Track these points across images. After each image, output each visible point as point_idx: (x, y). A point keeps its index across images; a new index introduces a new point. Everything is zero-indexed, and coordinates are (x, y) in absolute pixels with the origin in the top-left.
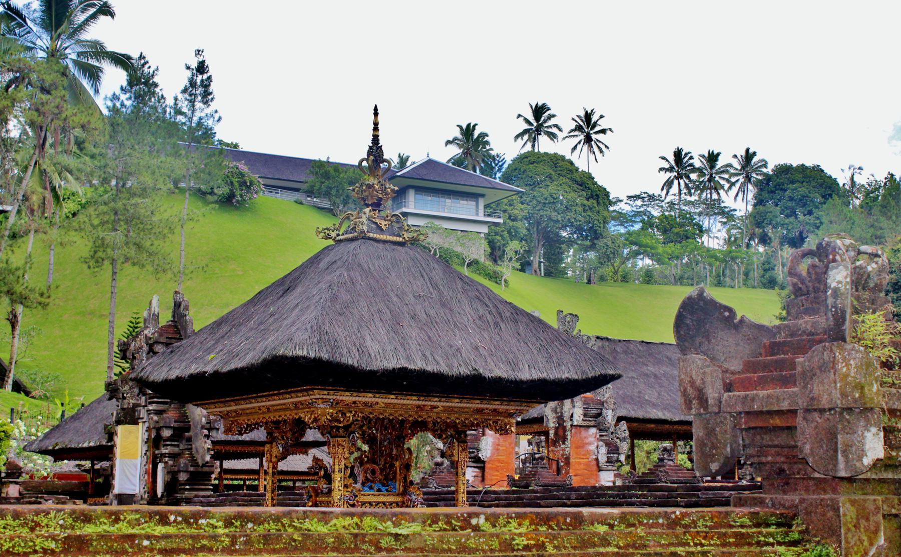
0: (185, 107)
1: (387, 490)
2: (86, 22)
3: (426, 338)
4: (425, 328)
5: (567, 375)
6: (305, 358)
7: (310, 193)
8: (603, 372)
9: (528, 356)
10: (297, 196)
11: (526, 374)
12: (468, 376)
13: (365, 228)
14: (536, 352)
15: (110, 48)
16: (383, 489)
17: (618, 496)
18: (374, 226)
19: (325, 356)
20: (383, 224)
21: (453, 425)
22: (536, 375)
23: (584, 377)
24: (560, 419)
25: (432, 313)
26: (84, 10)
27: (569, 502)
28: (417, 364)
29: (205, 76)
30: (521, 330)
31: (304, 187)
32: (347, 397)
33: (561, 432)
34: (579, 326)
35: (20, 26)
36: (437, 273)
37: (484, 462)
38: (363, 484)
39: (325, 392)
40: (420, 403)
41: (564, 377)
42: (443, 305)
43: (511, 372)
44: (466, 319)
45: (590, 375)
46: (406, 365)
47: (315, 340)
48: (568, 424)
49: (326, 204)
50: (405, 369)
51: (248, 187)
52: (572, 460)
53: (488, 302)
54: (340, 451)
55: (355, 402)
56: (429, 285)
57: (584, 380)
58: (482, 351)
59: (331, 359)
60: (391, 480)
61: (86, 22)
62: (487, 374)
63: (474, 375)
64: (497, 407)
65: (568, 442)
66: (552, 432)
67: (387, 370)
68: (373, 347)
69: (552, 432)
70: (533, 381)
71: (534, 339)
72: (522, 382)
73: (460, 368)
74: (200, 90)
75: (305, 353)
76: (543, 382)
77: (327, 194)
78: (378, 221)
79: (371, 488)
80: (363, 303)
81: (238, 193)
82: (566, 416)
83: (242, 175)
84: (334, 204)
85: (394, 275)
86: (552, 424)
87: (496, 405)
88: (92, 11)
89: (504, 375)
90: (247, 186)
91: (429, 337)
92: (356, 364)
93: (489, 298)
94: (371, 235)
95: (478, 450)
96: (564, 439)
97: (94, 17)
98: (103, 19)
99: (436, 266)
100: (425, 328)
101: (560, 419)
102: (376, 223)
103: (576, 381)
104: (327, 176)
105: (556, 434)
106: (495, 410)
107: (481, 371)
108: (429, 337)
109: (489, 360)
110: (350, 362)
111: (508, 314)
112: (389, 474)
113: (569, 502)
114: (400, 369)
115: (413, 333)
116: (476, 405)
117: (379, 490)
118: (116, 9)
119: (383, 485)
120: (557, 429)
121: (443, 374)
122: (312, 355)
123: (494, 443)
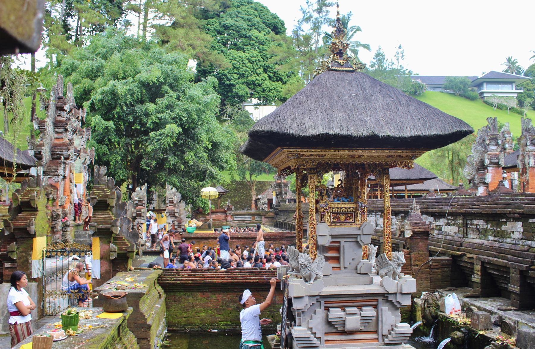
0: (395, 61)
1: (348, 201)
2: (352, 35)
3: (347, 117)
4: (349, 112)
5: (435, 133)
6: (262, 131)
7: (446, 88)
8: (459, 130)
9: (411, 123)
10: (440, 90)
11: (407, 133)
12: (368, 136)
13: (330, 65)
14: (416, 121)
15: (362, 43)
16: (346, 200)
17: (510, 199)
18: (336, 64)
19: (274, 129)
20: (342, 62)
21: (380, 165)
22: (414, 133)
23: (446, 133)
24: (524, 164)
25: (357, 103)
26: (352, 31)
27: (487, 203)
28: (336, 130)
29: (401, 50)
30: (411, 109)
31: (443, 86)
32: (306, 152)
33: (524, 170)
34: (531, 123)
35: (330, 39)
36: (367, 83)
37: (488, 184)
38: (334, 198)
39: (291, 150)
40: (351, 154)
41: (432, 134)
42: (366, 99)
43: (397, 133)
44: (378, 106)
45: (450, 132)
46: (327, 132)
47: (270, 121)
48: (527, 166)
49: (452, 92)
50: (326, 134)
51: (422, 88)
52: (530, 182)
53: (394, 97)
54: (312, 181)
55: (311, 155)
56: (360, 90)
57: (446, 135)
58: (381, 122)
59: (279, 130)
60: (351, 195)
61: (352, 35)
62: (381, 134)
63: (372, 136)
64: (400, 154)
65: (528, 174)
66: (521, 170)
67: (315, 135)
68: (308, 122)
69: (521, 170)
70: (411, 137)
71: (418, 114)
72: (404, 138)
73: (364, 132)
74: (400, 55)
75: (263, 128)
76: (418, 138)
77: (452, 88)
78: (339, 61)
79: (339, 200)
80: (313, 102)
81: (418, 91)
82: (526, 163)
83: (419, 84)
84: (455, 91)
85: (340, 86)
86: (520, 167)
87: (399, 152)
88: (354, 30)
89: (392, 134)
90: (421, 87)
91: (349, 116)
92: (294, 133)
93: (395, 94)
94: (334, 68)
95: (485, 179)
96: (526, 173)
97: (355, 32)
98: (357, 32)
99: (367, 80)
100: (349, 112)
101: (524, 164)
102: (338, 62)
103: (441, 136)
104: (451, 81)
105: (522, 171)
106: (399, 156)
107: (377, 133)
108: (349, 116)
109: (384, 126)
110: (291, 132)
111: (404, 101)
112: (349, 192)
113: (487, 203)
114: (323, 134)
115: (340, 115)
116: (387, 152)
117: (343, 201)
118: (361, 28)
119: (346, 198)
120: (523, 169)
121: (351, 136)
122: (266, 129)
123: (492, 176)
